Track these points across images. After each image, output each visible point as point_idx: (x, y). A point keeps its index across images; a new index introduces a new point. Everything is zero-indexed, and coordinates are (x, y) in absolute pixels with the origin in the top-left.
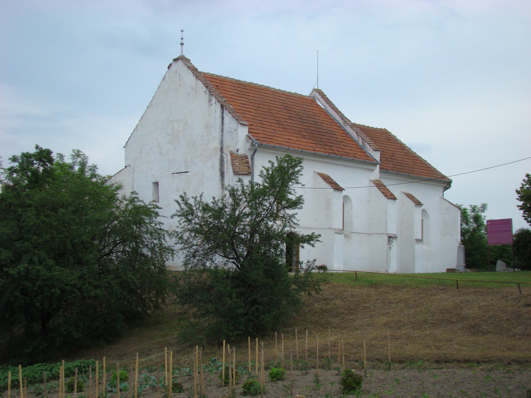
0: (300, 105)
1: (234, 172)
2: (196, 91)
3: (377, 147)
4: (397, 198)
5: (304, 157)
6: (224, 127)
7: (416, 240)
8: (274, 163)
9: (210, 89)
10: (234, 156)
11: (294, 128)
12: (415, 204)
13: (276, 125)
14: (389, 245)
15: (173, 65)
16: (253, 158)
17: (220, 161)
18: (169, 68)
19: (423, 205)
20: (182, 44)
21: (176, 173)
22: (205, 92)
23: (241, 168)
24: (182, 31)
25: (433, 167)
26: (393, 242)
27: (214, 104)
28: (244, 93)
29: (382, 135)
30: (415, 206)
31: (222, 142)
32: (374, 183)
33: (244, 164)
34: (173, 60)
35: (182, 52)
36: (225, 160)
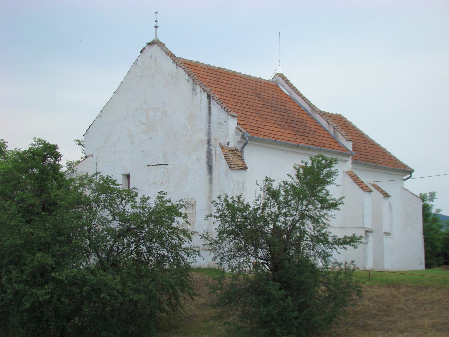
0: (268, 92)
1: (230, 167)
2: (177, 79)
3: (350, 137)
5: (339, 157)
6: (212, 118)
7: (385, 233)
8: (307, 163)
9: (193, 77)
10: (225, 150)
11: (272, 118)
12: (384, 195)
13: (256, 115)
14: (366, 240)
15: (146, 49)
16: (242, 151)
17: (207, 153)
18: (141, 52)
19: (391, 196)
20: (156, 27)
21: (153, 165)
22: (188, 80)
23: (236, 162)
24: (156, 13)
25: (393, 156)
27: (198, 94)
28: (218, 80)
29: (339, 121)
30: (383, 198)
31: (209, 134)
32: (348, 175)
33: (238, 158)
34: (148, 44)
35: (156, 36)
36: (213, 152)
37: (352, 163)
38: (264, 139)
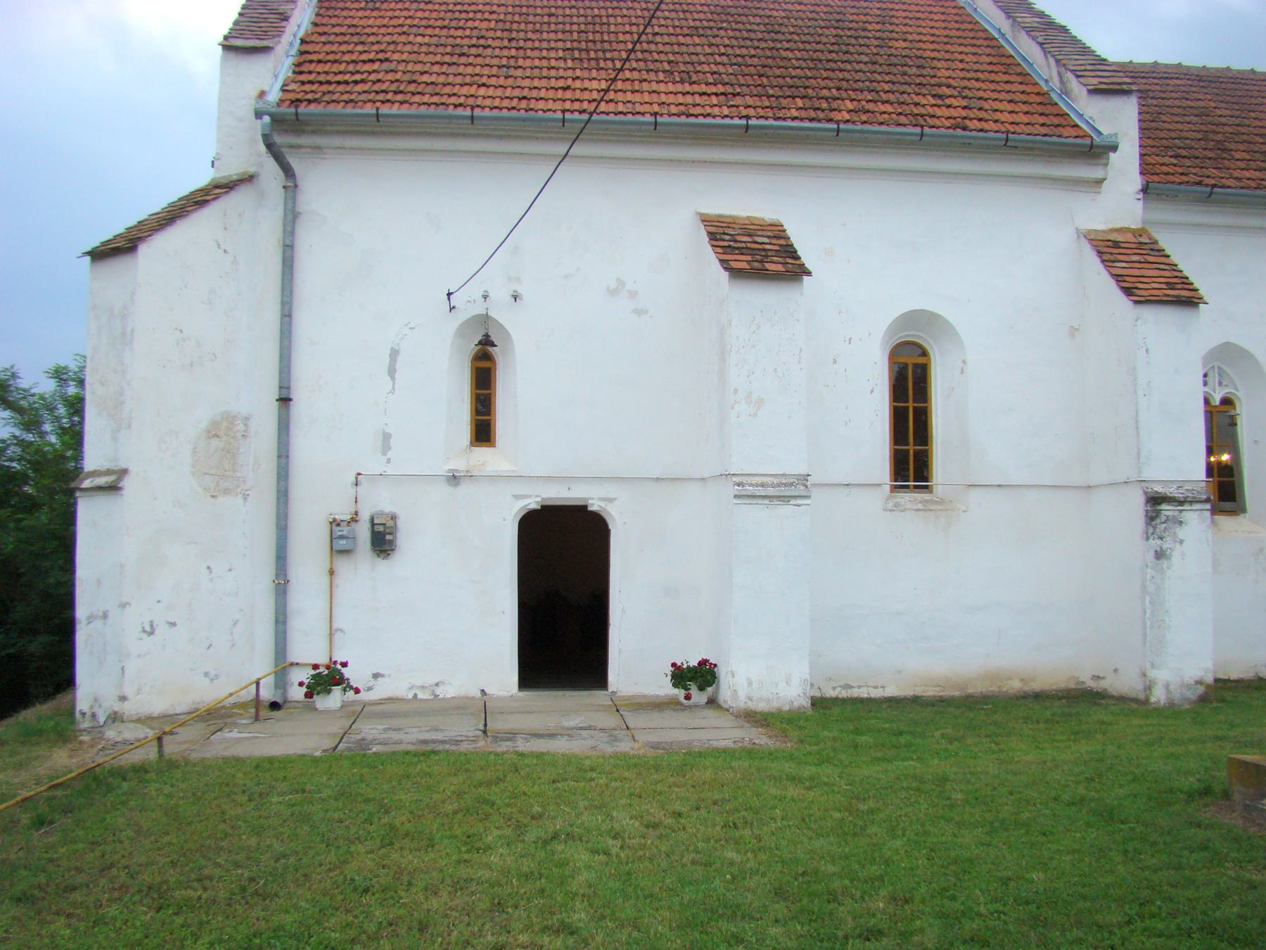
4: (1206, 299)
14: (1155, 543)
26: (1181, 523)
32: (1090, 240)
37: (1145, 190)
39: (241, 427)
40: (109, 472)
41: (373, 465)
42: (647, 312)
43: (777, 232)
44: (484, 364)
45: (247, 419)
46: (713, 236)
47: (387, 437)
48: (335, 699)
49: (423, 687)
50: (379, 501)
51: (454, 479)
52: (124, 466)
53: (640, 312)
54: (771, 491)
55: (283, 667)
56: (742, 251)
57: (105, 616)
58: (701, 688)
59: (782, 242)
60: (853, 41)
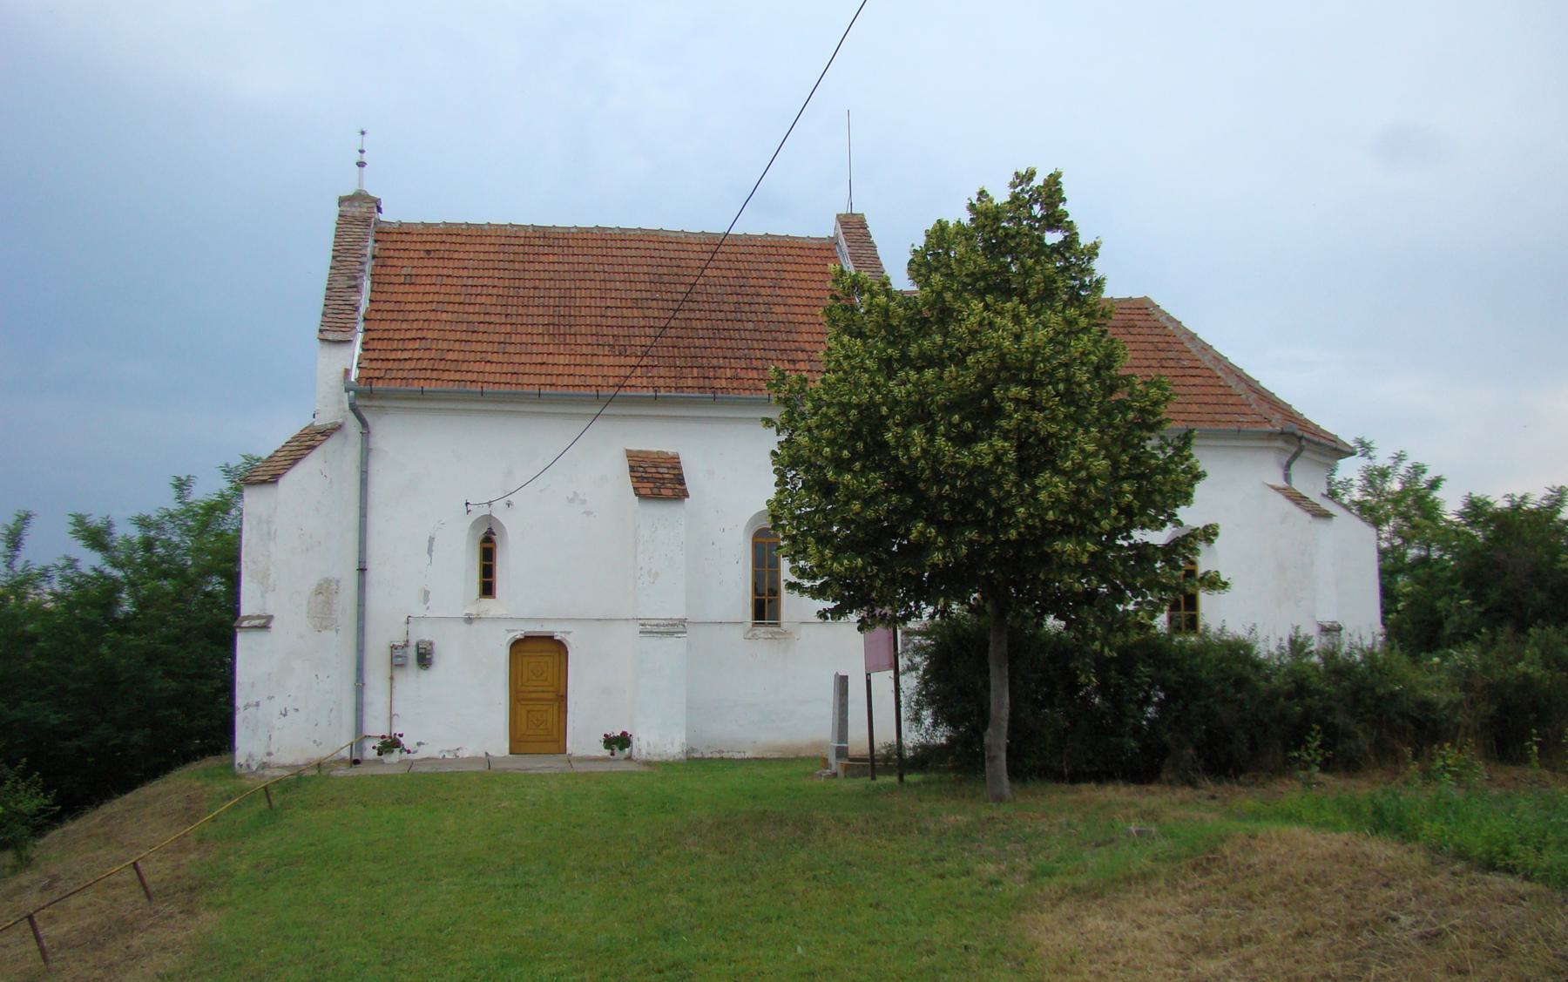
20: (361, 164)
24: (363, 133)
35: (360, 183)
38: (603, 396)
39: (335, 587)
40: (259, 617)
41: (418, 610)
42: (592, 513)
43: (674, 463)
44: (488, 545)
45: (338, 581)
46: (632, 469)
47: (427, 593)
48: (396, 756)
49: (449, 751)
50: (422, 633)
51: (469, 620)
52: (271, 614)
53: (588, 513)
54: (662, 629)
55: (360, 737)
56: (648, 480)
57: (257, 704)
58: (621, 749)
59: (676, 472)
60: (747, 308)
